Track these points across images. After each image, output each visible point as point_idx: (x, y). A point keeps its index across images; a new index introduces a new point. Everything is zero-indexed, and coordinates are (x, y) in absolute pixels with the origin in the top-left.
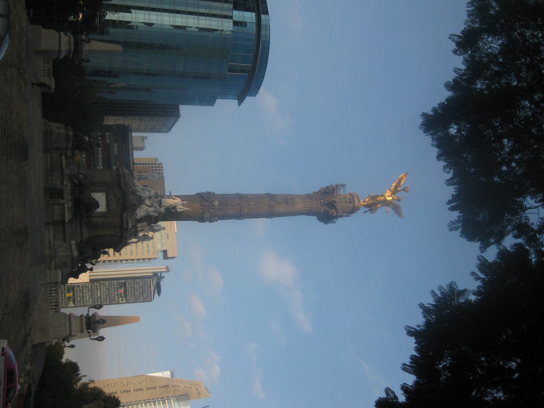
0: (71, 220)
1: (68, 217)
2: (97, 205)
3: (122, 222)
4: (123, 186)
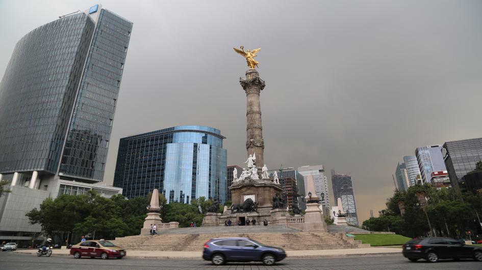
0: (258, 212)
1: (255, 214)
2: (249, 200)
3: (261, 187)
4: (240, 187)
